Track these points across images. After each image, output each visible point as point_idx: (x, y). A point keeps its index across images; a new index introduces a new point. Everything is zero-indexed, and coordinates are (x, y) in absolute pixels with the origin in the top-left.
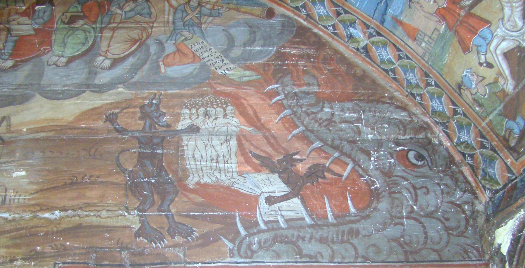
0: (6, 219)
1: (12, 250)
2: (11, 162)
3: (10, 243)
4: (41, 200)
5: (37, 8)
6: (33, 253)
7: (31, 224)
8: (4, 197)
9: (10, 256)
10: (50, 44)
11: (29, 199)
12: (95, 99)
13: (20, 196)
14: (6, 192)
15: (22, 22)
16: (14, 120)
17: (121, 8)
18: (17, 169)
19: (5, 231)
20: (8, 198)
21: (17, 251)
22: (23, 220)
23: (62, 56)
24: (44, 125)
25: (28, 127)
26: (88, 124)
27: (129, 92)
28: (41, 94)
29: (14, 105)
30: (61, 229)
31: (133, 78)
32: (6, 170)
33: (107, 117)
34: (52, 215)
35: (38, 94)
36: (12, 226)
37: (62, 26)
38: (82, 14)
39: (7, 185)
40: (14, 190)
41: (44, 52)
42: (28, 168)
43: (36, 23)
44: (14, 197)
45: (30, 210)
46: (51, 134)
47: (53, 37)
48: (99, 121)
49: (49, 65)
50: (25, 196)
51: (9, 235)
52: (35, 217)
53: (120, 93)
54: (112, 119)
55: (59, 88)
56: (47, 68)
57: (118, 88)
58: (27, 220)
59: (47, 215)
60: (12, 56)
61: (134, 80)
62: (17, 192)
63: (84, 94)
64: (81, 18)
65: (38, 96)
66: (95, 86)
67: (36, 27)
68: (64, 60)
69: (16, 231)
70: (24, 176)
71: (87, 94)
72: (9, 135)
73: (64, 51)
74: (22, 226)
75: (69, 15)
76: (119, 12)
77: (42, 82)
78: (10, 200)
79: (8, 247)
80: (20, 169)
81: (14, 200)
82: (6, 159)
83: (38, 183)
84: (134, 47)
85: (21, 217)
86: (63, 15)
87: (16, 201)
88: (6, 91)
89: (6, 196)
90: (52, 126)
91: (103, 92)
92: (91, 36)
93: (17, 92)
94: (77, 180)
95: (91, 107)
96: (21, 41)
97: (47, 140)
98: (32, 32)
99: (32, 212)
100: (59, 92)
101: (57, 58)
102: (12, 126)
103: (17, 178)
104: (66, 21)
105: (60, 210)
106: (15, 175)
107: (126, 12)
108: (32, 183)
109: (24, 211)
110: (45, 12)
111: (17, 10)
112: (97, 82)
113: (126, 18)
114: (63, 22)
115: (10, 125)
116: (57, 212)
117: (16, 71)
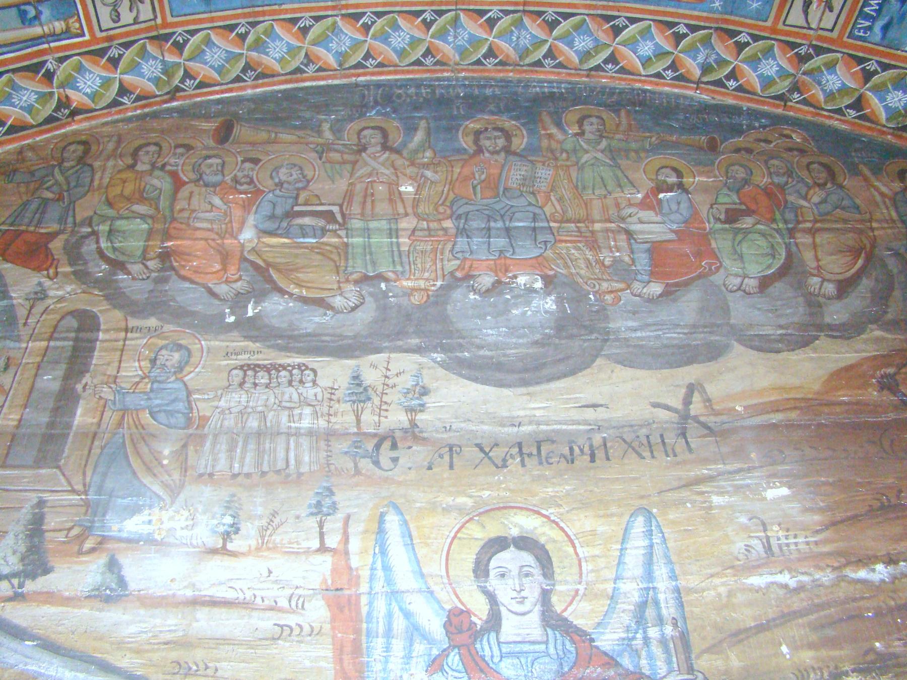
0: (785, 586)
1: (824, 653)
2: (749, 470)
3: (813, 637)
4: (842, 545)
5: (661, 196)
6: (871, 657)
7: (841, 594)
8: (765, 541)
9: (828, 667)
10: (713, 255)
11: (816, 543)
12: (843, 350)
13: (795, 537)
14: (765, 530)
15: (645, 219)
16: (712, 390)
17: (805, 198)
18: (769, 483)
19: (795, 612)
20: (773, 542)
21: (836, 653)
22: (820, 586)
23: (745, 276)
24: (773, 398)
25: (745, 403)
26: (850, 396)
27: (893, 337)
28: (740, 342)
29: (699, 363)
30: (903, 602)
31: (885, 312)
32: (748, 486)
33: (878, 381)
34: (872, 574)
35: (735, 344)
36: (802, 600)
37: (719, 226)
38: (744, 207)
39: (763, 517)
40: (779, 525)
41: (710, 269)
42: (790, 480)
43: (673, 222)
44: (784, 541)
45: (828, 566)
46: (793, 415)
47: (714, 245)
48: (870, 390)
49: (731, 292)
50: (806, 537)
51: (805, 620)
52: (843, 578)
53: (877, 340)
54: (888, 385)
55: (768, 331)
56: (730, 297)
57: (872, 330)
58: (827, 587)
59: (862, 574)
60: (655, 274)
61: (889, 316)
62: (788, 530)
63: (817, 342)
64: (749, 212)
65: (738, 348)
66: (831, 327)
67: (675, 227)
68: (751, 284)
69: (817, 611)
70: (788, 496)
71: (823, 342)
72: (718, 419)
73: (744, 268)
74: (824, 599)
75: (722, 208)
76: (803, 203)
77: (732, 321)
78: (780, 546)
79: (811, 646)
80: (774, 483)
81: (788, 545)
82: (736, 466)
83: (821, 510)
84: (860, 262)
85: (813, 581)
86: (711, 207)
87: (793, 547)
88: (675, 338)
89: (768, 538)
90: (788, 399)
91: (849, 338)
92: (778, 243)
93: (696, 340)
94: (888, 500)
95: (842, 364)
96: (656, 250)
97: (790, 426)
98: (672, 236)
99: (834, 569)
100: (773, 337)
101: (739, 280)
102: (713, 401)
103: (775, 501)
104: (722, 217)
105: (884, 563)
106: (771, 494)
107: (815, 204)
108: (806, 510)
109: (818, 568)
110: (679, 203)
111: (629, 200)
112: (828, 320)
113: (821, 215)
114: (718, 220)
115: (708, 401)
116: (880, 567)
117: (674, 301)
